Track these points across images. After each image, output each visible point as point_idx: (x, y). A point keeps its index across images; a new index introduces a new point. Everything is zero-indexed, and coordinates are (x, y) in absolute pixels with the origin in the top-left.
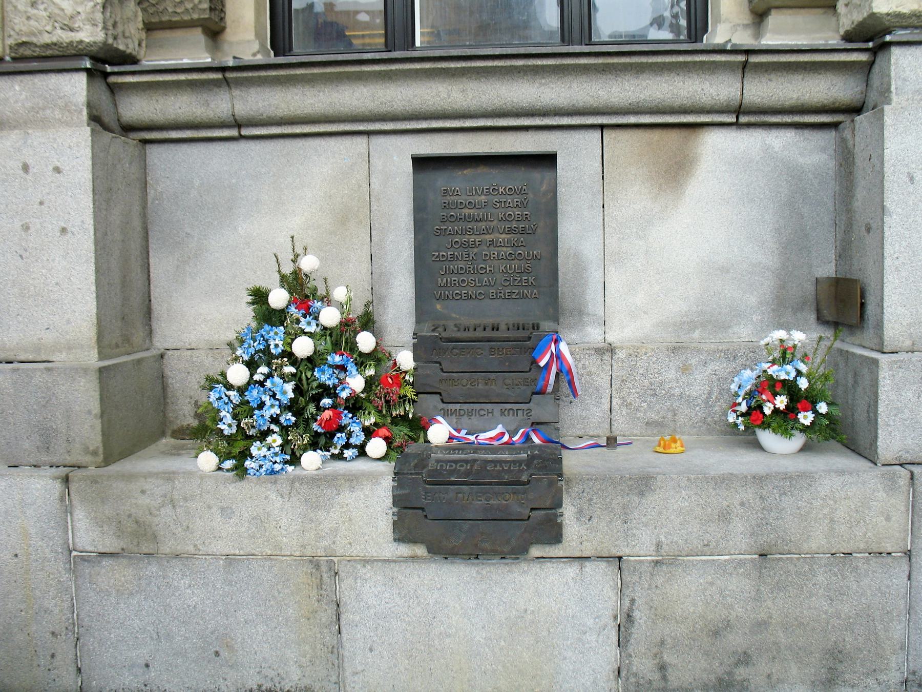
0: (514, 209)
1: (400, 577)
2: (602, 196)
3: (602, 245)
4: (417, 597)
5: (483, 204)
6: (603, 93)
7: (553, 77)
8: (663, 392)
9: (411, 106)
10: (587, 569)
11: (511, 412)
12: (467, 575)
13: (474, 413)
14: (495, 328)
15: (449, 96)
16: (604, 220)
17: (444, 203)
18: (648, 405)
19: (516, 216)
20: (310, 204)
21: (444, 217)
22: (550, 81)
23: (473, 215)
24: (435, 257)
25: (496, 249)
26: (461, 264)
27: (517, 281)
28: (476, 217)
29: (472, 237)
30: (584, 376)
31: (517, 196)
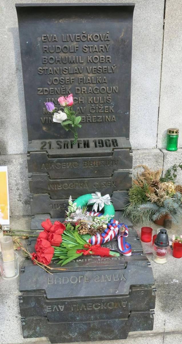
0: (99, 53)
2: (161, 43)
5: (76, 49)
10: (167, 339)
16: (162, 61)
17: (45, 48)
19: (101, 59)
21: (45, 60)
23: (68, 58)
24: (40, 91)
25: (85, 85)
28: (70, 59)
29: (67, 76)
31: (102, 42)
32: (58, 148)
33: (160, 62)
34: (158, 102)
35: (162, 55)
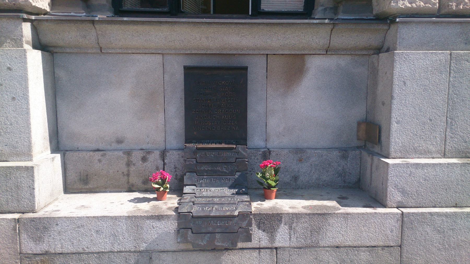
1: (180, 259)
12: (210, 256)
19: (230, 94)
20: (136, 85)
30: (258, 163)
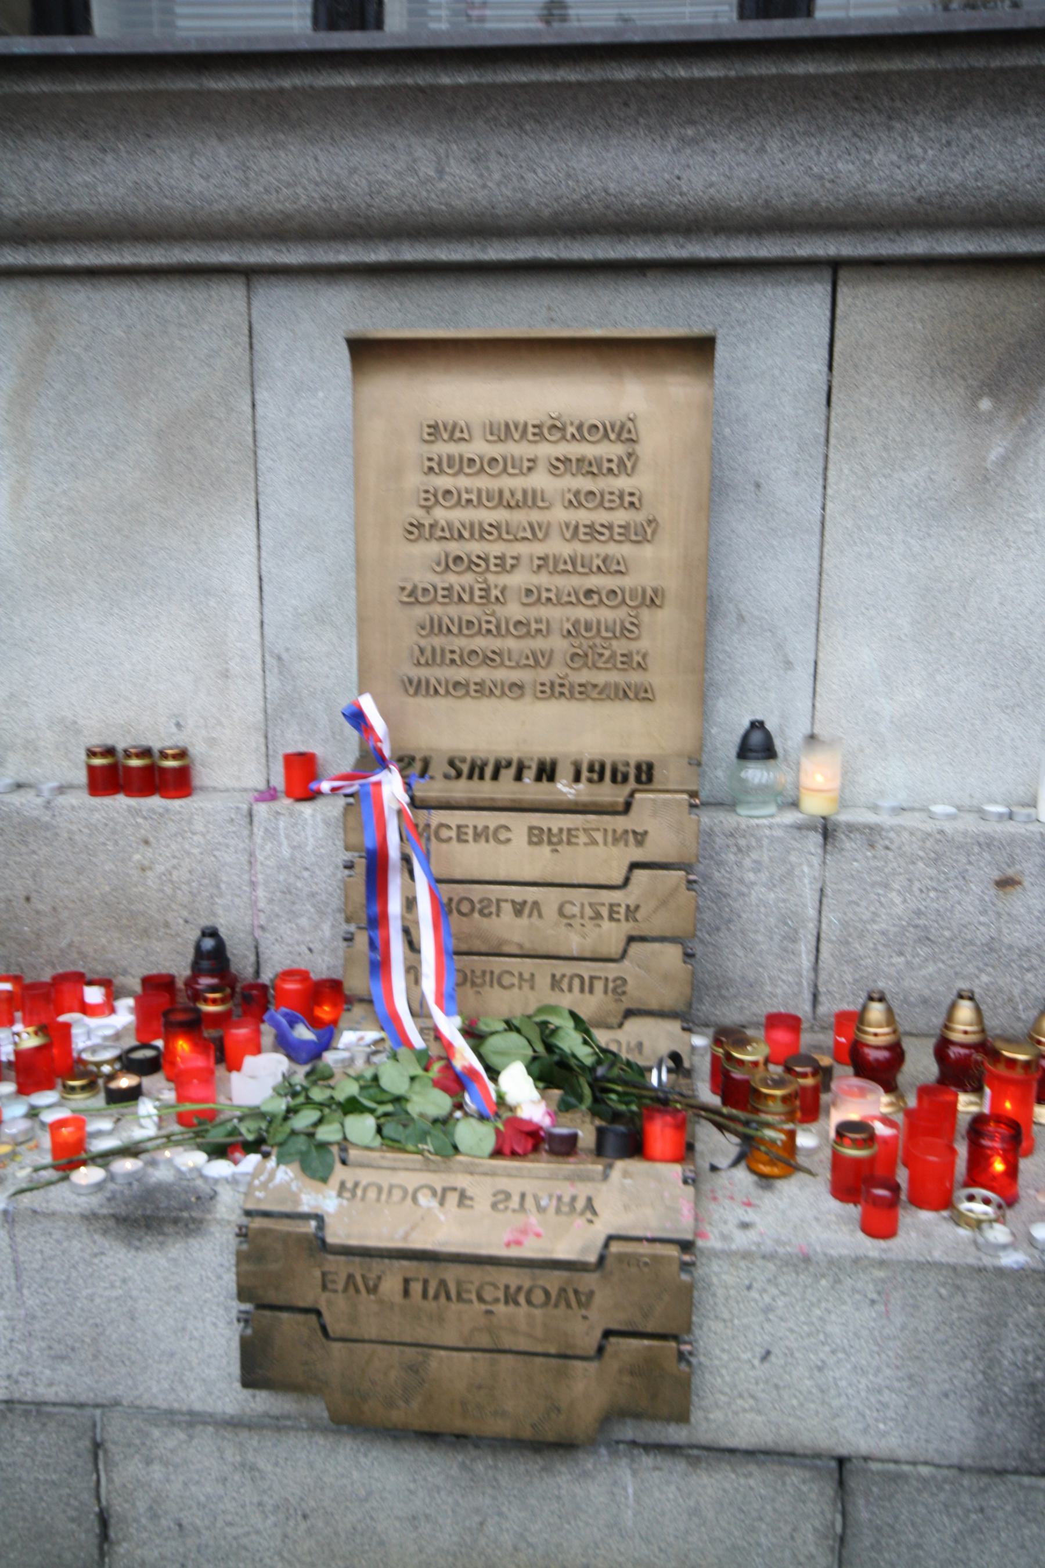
2: (821, 449)
3: (816, 572)
4: (305, 1517)
6: (851, 167)
7: (716, 118)
8: (947, 933)
9: (344, 198)
11: (576, 982)
13: (488, 978)
14: (547, 772)
15: (441, 172)
16: (824, 509)
18: (908, 963)
19: (607, 497)
22: (710, 133)
23: (501, 493)
26: (470, 612)
27: (604, 659)
30: (756, 888)
32: (447, 777)
33: (819, 510)
34: (811, 644)
35: (825, 487)
